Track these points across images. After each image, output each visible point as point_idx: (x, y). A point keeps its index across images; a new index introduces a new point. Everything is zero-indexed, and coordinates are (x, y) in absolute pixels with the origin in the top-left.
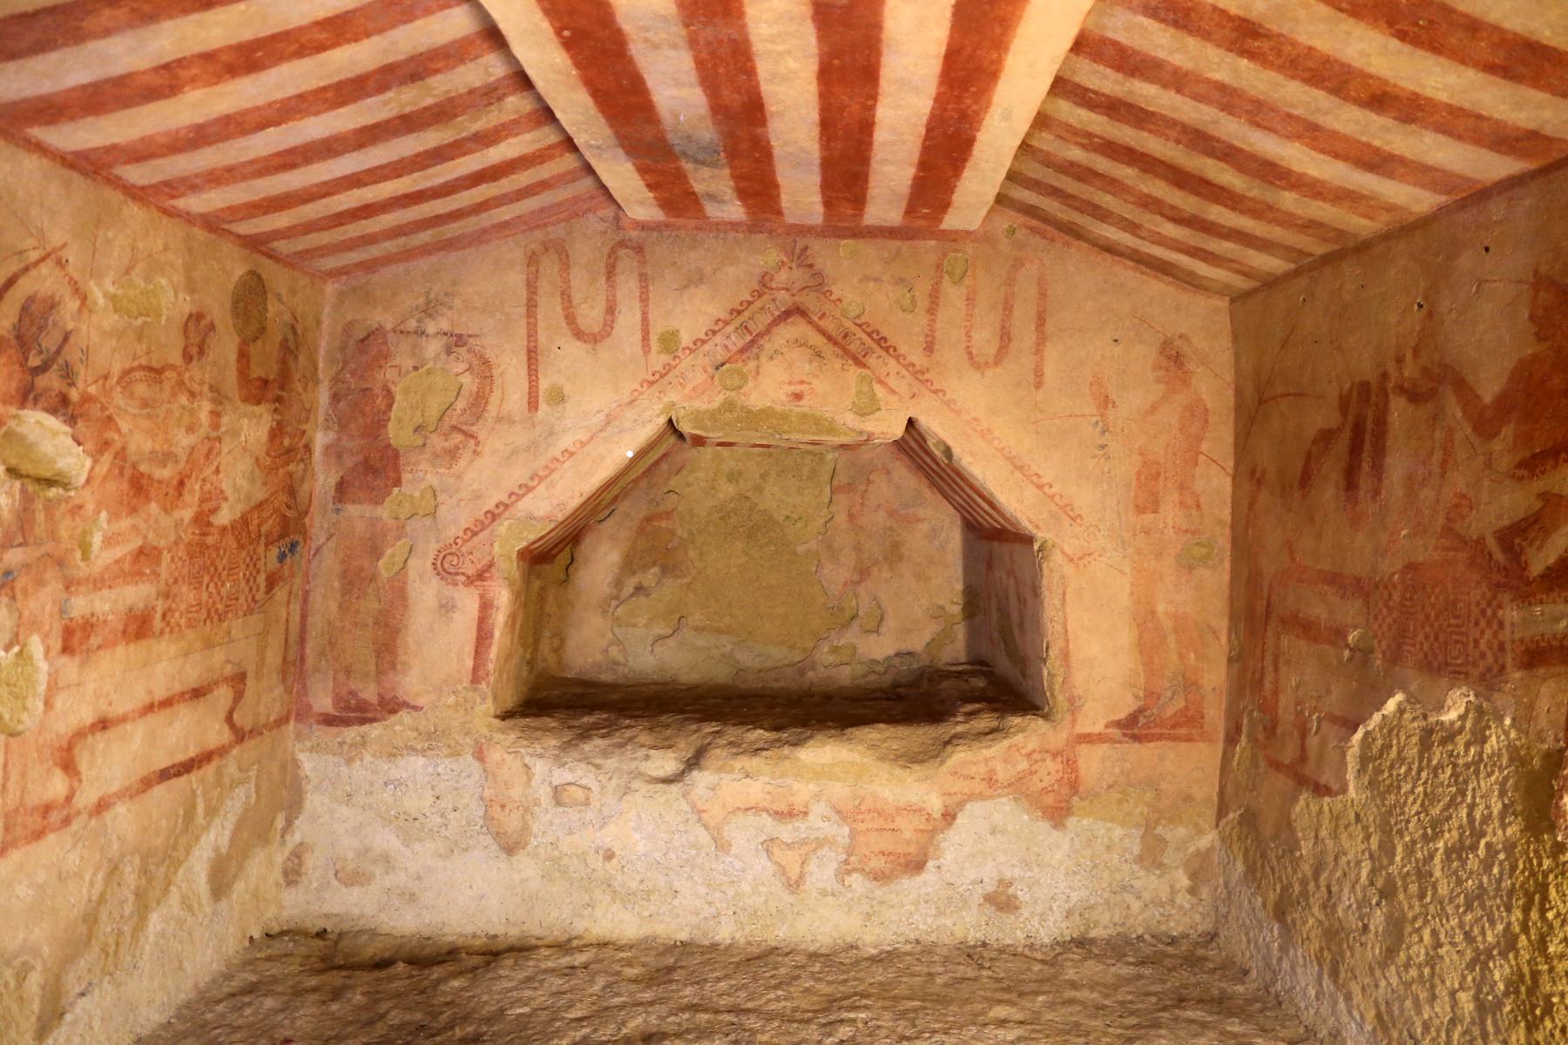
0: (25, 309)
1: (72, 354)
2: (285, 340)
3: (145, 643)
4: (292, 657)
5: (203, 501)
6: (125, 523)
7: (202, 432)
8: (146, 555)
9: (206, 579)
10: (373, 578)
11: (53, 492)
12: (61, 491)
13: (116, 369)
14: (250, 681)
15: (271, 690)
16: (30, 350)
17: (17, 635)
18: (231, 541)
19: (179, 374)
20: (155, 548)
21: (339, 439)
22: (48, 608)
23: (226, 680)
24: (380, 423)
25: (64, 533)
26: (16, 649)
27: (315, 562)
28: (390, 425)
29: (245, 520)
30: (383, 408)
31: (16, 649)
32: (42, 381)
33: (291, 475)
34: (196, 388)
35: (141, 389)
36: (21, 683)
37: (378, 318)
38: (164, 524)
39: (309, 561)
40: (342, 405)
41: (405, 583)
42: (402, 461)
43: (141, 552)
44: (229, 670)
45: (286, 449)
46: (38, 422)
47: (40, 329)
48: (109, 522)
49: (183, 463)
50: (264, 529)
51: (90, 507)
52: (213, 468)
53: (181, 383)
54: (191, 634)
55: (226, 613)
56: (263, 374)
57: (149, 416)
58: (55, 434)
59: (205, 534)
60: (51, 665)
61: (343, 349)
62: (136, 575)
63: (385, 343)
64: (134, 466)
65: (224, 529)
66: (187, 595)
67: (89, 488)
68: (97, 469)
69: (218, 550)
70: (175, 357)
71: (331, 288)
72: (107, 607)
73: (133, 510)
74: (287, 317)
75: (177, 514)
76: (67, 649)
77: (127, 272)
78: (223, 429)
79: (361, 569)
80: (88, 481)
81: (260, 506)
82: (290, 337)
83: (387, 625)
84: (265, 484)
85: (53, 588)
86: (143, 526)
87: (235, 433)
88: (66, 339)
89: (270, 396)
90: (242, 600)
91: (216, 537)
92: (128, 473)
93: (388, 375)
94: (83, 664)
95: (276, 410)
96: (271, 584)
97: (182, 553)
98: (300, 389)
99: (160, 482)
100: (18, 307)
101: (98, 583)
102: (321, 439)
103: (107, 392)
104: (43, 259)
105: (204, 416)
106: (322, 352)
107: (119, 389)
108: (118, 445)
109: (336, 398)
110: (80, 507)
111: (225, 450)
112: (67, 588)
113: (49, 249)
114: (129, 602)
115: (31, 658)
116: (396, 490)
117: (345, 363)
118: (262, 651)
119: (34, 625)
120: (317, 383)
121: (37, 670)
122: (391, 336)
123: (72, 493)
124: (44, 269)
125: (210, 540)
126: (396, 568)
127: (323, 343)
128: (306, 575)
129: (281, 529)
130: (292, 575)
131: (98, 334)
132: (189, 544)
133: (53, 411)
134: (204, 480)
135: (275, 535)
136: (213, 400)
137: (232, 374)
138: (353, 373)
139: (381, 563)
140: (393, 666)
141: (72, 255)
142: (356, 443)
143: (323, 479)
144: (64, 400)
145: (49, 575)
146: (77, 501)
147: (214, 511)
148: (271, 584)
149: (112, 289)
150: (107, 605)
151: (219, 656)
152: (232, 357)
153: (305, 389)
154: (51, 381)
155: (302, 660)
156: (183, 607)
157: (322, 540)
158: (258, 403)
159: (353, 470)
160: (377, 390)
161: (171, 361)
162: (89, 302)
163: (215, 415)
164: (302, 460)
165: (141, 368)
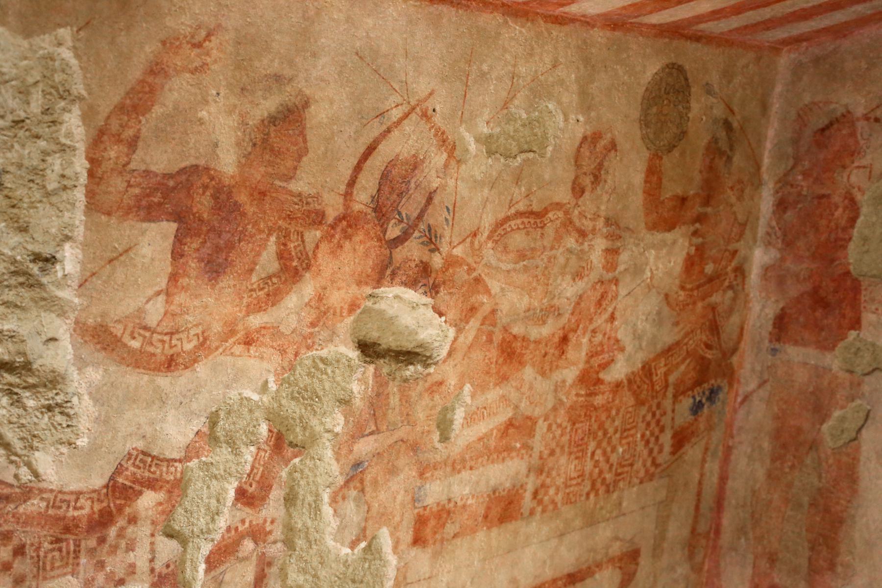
0: (385, 176)
1: (436, 217)
2: (715, 140)
3: (511, 526)
4: (702, 527)
5: (591, 355)
6: (493, 395)
7: (594, 276)
8: (518, 428)
9: (592, 445)
10: (814, 445)
11: (410, 371)
12: (419, 367)
13: (487, 221)
14: (644, 561)
15: (672, 569)
16: (389, 220)
17: (364, 530)
18: (629, 400)
19: (566, 213)
20: (529, 418)
21: (783, 259)
22: (400, 498)
23: (611, 560)
24: (840, 243)
25: (420, 414)
26: (363, 545)
27: (741, 413)
28: (852, 246)
29: (647, 370)
30: (843, 223)
31: (363, 545)
32: (400, 254)
33: (713, 308)
34: (588, 224)
35: (518, 240)
36: (369, 578)
37: (845, 101)
38: (540, 390)
39: (735, 411)
40: (789, 215)
41: (856, 459)
42: (864, 296)
43: (510, 424)
44: (616, 549)
45: (709, 277)
46: (396, 297)
47: (400, 195)
48: (473, 396)
49: (567, 316)
50: (672, 379)
51: (452, 381)
52: (606, 316)
53: (568, 223)
54: (568, 512)
55: (616, 482)
56: (679, 191)
57: (526, 269)
58: (414, 307)
59: (591, 394)
60: (400, 558)
61: (795, 142)
62: (503, 451)
63: (853, 134)
64: (505, 329)
65: (618, 385)
66: (566, 466)
67: (451, 362)
68: (461, 339)
69: (608, 410)
70: (563, 194)
71: (785, 61)
72: (467, 491)
73: (504, 379)
74: (719, 111)
75: (557, 376)
76: (418, 541)
77: (505, 106)
78: (621, 268)
79: (799, 430)
80: (450, 354)
81: (668, 351)
82: (722, 134)
83: (827, 510)
84: (677, 324)
85: (408, 474)
86: (514, 395)
87: (637, 270)
88: (430, 200)
89: (690, 214)
90: (638, 465)
91: (608, 396)
92: (498, 337)
93: (853, 179)
94: (436, 555)
95: (695, 233)
96: (681, 440)
97: (562, 417)
98: (733, 199)
99: (537, 342)
100: (377, 175)
101: (456, 466)
102: (759, 257)
103: (476, 252)
104: (406, 116)
105: (597, 257)
106: (768, 145)
107: (490, 244)
108: (486, 309)
109: (781, 205)
110: (441, 383)
111: (623, 292)
112: (421, 475)
113: (413, 103)
114: (492, 482)
115: (379, 551)
116: (853, 334)
117: (797, 160)
118: (662, 522)
119: (384, 517)
120: (758, 184)
121: (385, 564)
122: (861, 125)
123: (431, 370)
124: (408, 127)
125: (599, 400)
126: (846, 437)
127: (771, 133)
128: (730, 425)
129: (702, 372)
130: (710, 428)
131: (469, 192)
132: (572, 408)
133: (412, 284)
134: (594, 331)
135: (689, 383)
136: (610, 237)
137: (637, 200)
138: (806, 174)
139: (825, 427)
140: (832, 567)
141: (440, 105)
142: (804, 267)
143: (759, 308)
144: (425, 269)
145: (402, 462)
146: (438, 378)
147: (604, 366)
148: (681, 440)
149: (486, 130)
150: (464, 489)
151: (604, 533)
152: (638, 179)
153: (740, 198)
154: (412, 251)
155: (718, 532)
156: (560, 481)
157: (752, 386)
158: (670, 227)
159: (798, 300)
160: (836, 199)
161: (556, 199)
162: (457, 153)
163: (612, 252)
164: (731, 287)
165: (519, 214)
